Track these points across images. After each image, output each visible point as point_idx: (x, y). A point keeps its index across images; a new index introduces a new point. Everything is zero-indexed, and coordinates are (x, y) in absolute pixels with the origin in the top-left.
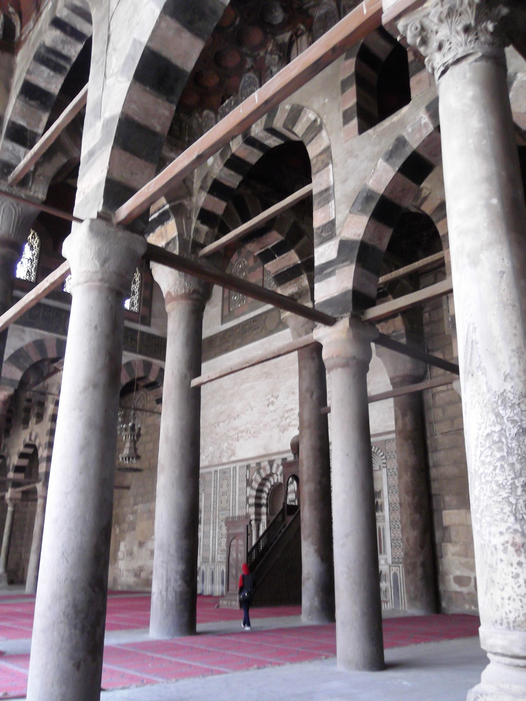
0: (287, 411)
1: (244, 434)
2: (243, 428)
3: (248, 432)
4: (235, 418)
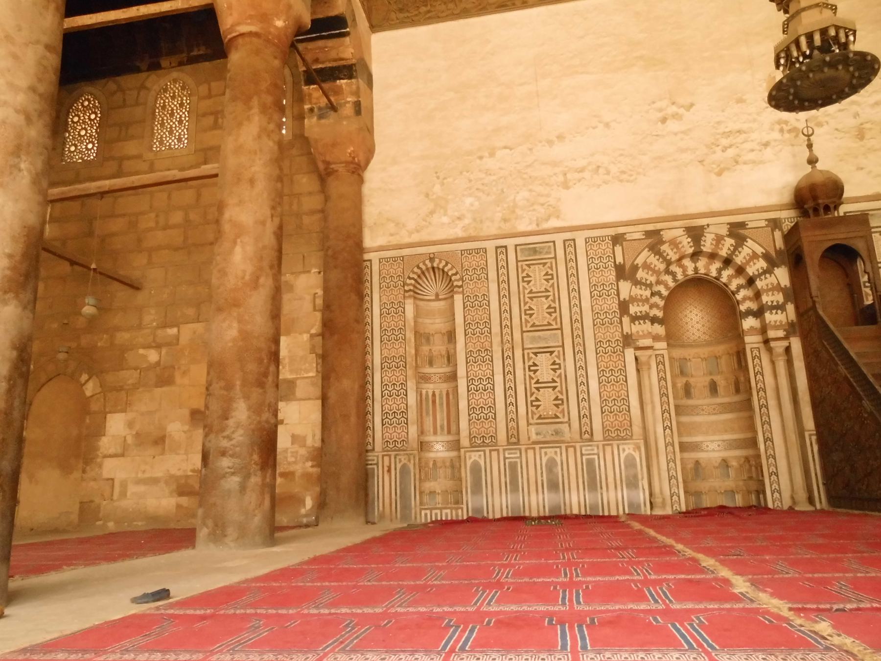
0: (727, 134)
1: (586, 175)
2: (582, 163)
3: (601, 171)
4: (550, 143)
